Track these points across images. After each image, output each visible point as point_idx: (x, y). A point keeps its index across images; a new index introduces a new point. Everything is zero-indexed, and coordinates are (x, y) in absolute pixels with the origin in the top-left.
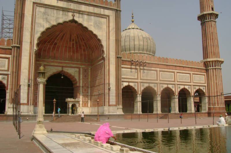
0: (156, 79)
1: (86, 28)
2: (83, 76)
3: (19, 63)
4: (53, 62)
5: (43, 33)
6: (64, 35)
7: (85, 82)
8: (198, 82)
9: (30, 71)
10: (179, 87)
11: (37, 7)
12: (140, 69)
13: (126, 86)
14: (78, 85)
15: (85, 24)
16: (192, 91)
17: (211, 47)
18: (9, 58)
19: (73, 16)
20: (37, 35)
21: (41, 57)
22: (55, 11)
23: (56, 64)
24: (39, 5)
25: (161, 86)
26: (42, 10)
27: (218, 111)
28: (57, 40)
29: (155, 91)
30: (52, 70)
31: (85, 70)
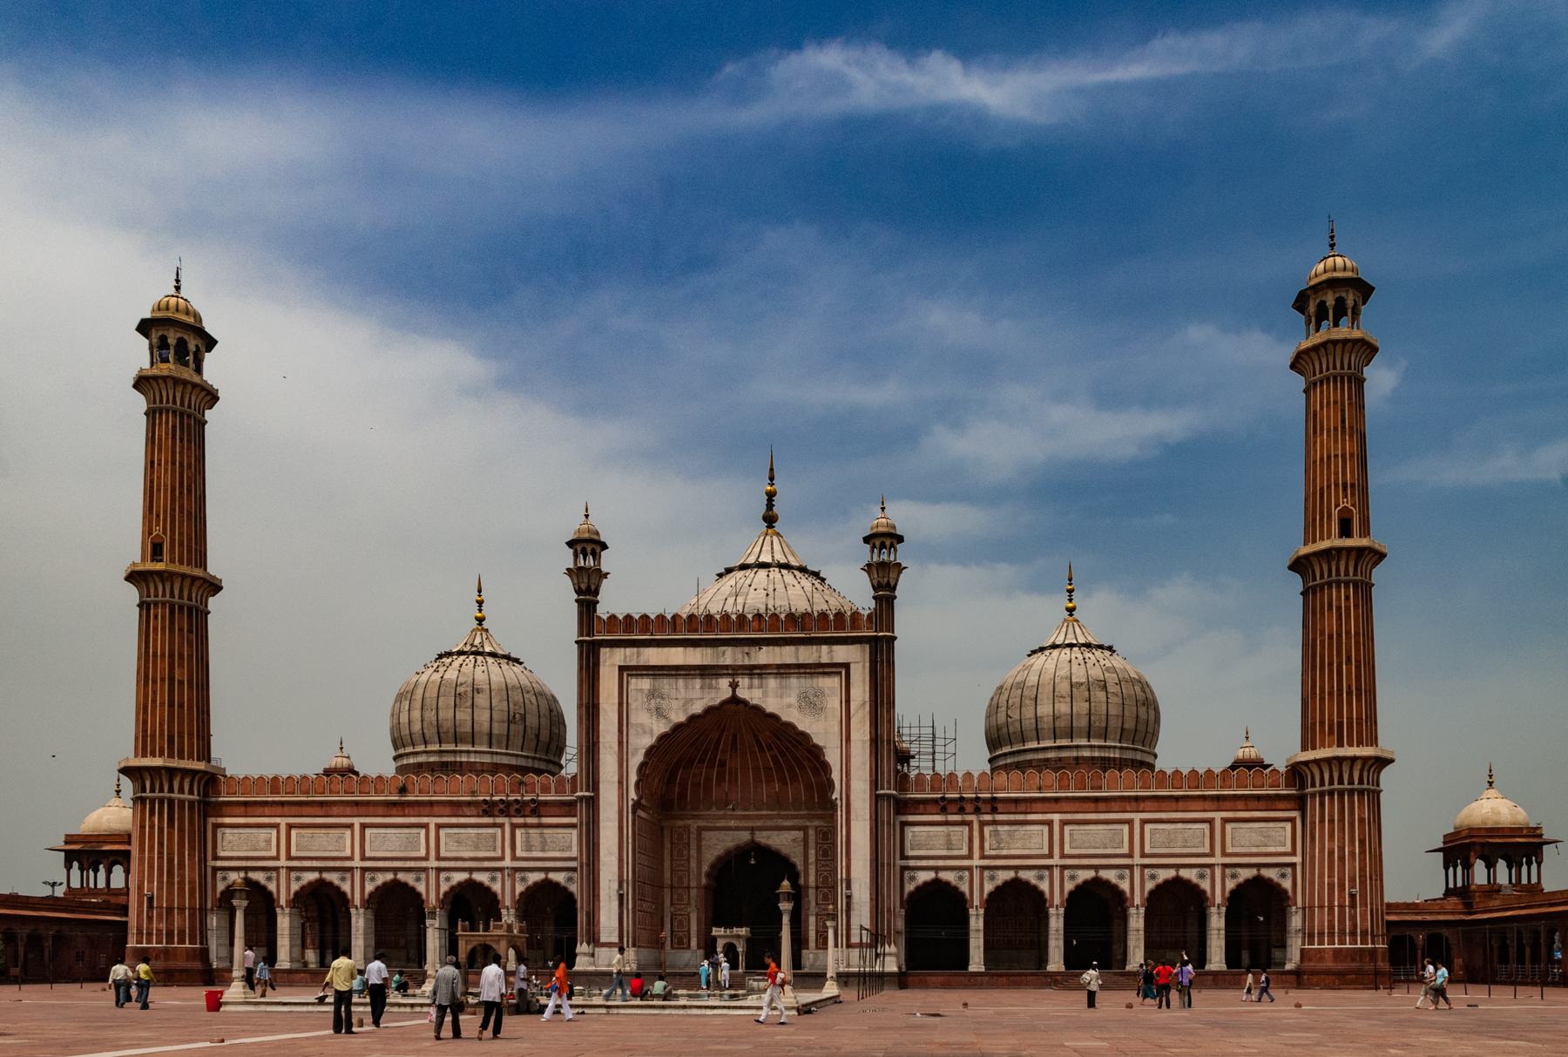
0: (1046, 851)
2: (816, 853)
3: (595, 840)
4: (723, 817)
5: (650, 752)
6: (735, 736)
7: (825, 871)
8: (1254, 850)
9: (623, 860)
10: (1153, 877)
12: (982, 824)
13: (926, 884)
15: (771, 706)
16: (1218, 889)
19: (734, 686)
20: (636, 760)
21: (689, 806)
22: (681, 682)
23: (732, 823)
24: (634, 672)
25: (1066, 878)
26: (645, 684)
27: (1329, 964)
28: (723, 752)
29: (1042, 894)
30: (718, 843)
31: (825, 834)
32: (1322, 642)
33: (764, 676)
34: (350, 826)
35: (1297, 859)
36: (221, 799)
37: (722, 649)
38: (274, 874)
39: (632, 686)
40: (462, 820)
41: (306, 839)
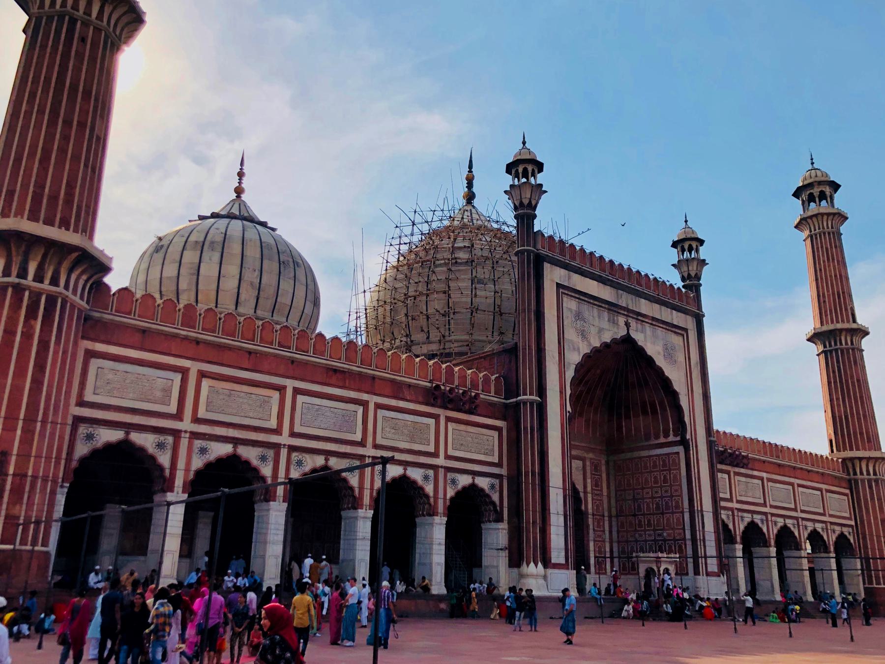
1: (650, 361)
2: (591, 482)
5: (579, 368)
8: (838, 514)
11: (563, 295)
14: (583, 508)
17: (859, 419)
18: (502, 428)
19: (627, 325)
20: (570, 374)
22: (596, 311)
24: (566, 292)
32: (853, 383)
33: (644, 323)
34: (281, 389)
35: (853, 523)
36: (111, 317)
37: (620, 292)
38: (170, 439)
39: (564, 305)
40: (402, 404)
41: (221, 397)
